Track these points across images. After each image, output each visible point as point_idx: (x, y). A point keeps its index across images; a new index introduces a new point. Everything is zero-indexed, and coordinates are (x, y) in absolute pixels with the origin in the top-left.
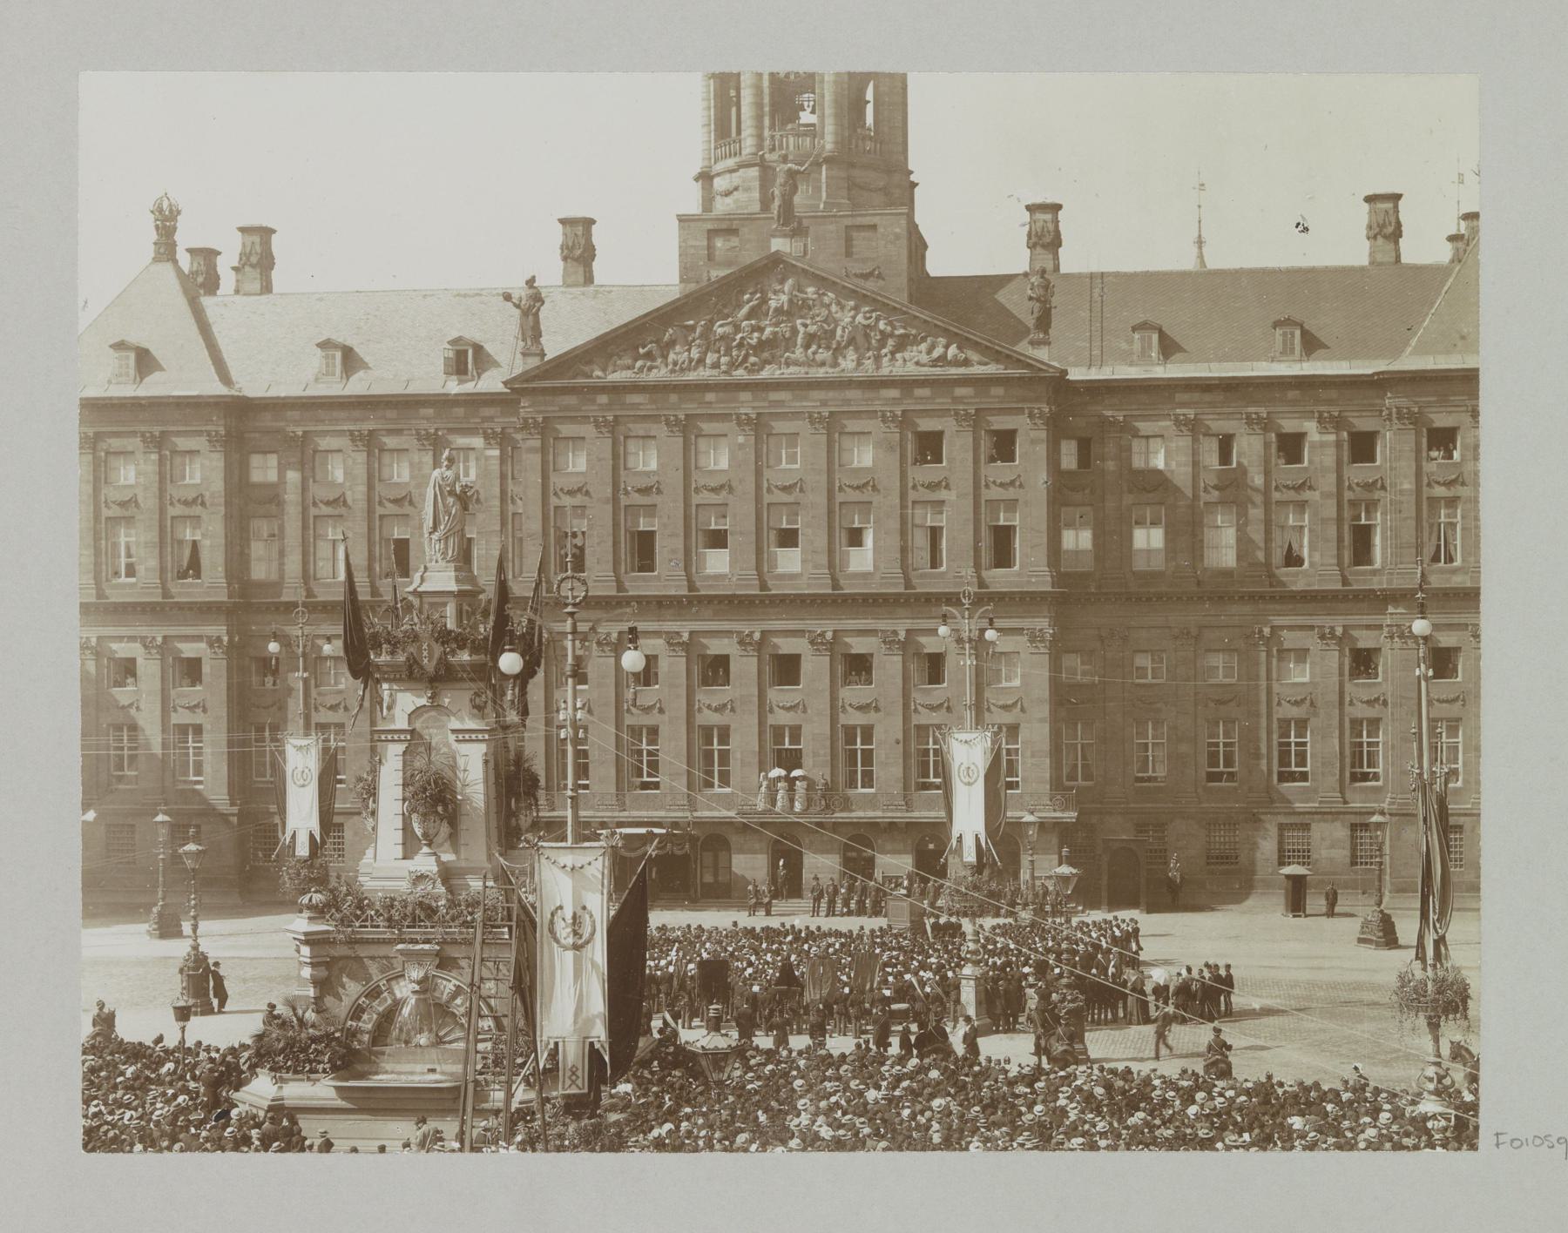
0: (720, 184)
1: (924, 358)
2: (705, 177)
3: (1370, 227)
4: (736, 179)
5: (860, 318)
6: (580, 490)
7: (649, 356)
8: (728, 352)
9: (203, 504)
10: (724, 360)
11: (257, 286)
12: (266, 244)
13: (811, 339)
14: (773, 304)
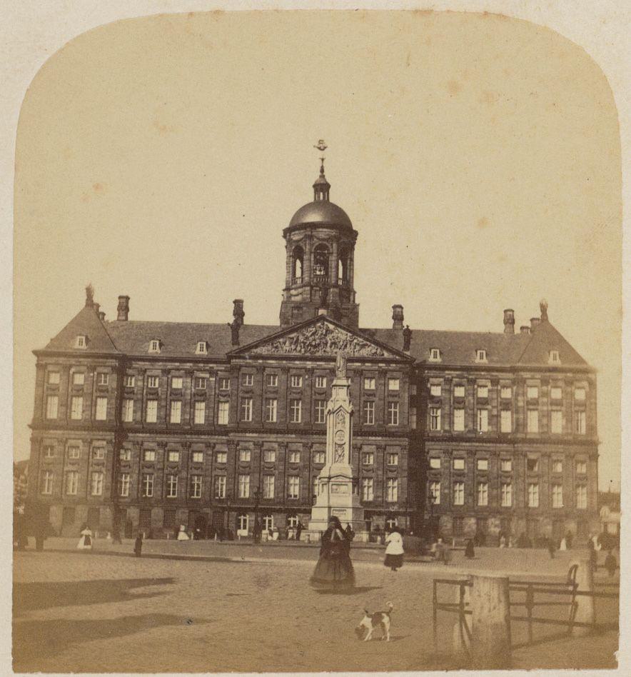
0: (293, 292)
2: (287, 289)
3: (504, 320)
4: (300, 290)
5: (348, 338)
7: (277, 347)
8: (304, 347)
9: (108, 392)
10: (303, 350)
11: (124, 318)
12: (127, 303)
13: (332, 343)
14: (320, 332)
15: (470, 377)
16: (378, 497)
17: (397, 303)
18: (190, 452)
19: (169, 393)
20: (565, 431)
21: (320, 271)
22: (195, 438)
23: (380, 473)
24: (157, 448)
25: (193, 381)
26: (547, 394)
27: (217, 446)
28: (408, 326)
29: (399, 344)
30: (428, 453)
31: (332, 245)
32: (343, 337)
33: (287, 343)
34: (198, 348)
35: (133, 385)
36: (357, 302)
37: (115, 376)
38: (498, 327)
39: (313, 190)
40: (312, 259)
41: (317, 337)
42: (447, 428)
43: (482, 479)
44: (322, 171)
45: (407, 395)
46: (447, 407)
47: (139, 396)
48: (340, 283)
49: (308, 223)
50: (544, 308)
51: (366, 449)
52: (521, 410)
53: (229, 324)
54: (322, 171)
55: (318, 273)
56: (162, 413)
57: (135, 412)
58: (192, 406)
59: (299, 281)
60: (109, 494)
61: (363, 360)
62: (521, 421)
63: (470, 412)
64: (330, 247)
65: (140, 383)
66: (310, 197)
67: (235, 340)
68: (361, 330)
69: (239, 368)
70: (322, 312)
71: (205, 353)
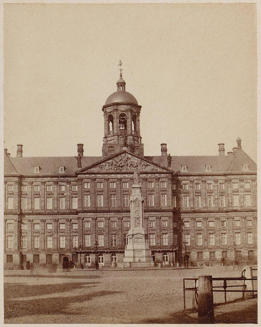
0: (109, 139)
1: (150, 169)
2: (106, 137)
4: (112, 138)
5: (139, 162)
6: (88, 191)
10: (115, 169)
11: (20, 155)
15: (203, 179)
16: (158, 243)
17: (163, 143)
18: (58, 224)
19: (45, 194)
20: (253, 205)
21: (122, 127)
22: (60, 217)
23: (159, 231)
24: (40, 222)
25: (58, 187)
26: (243, 186)
27: (72, 220)
28: (169, 154)
29: (165, 164)
30: (183, 219)
31: (128, 114)
32: (136, 161)
33: (107, 166)
34: (60, 170)
35: (26, 191)
36: (142, 143)
37: (17, 186)
38: (216, 153)
39: (116, 86)
40: (118, 121)
41: (122, 162)
42: (192, 206)
43: (212, 232)
44: (121, 76)
45: (171, 190)
46: (192, 195)
47: (30, 196)
48: (133, 133)
49: (115, 103)
50: (239, 142)
51: (150, 219)
52: (230, 195)
53: (76, 157)
54: (121, 76)
55: (121, 128)
56: (43, 204)
57: (28, 204)
58: (58, 200)
59: (112, 133)
60: (16, 248)
61: (146, 173)
62: (230, 201)
63: (204, 197)
64: (127, 115)
65: (30, 189)
66: (115, 89)
67: (79, 165)
68: (145, 157)
69: (82, 180)
70: (125, 148)
71: (63, 172)
